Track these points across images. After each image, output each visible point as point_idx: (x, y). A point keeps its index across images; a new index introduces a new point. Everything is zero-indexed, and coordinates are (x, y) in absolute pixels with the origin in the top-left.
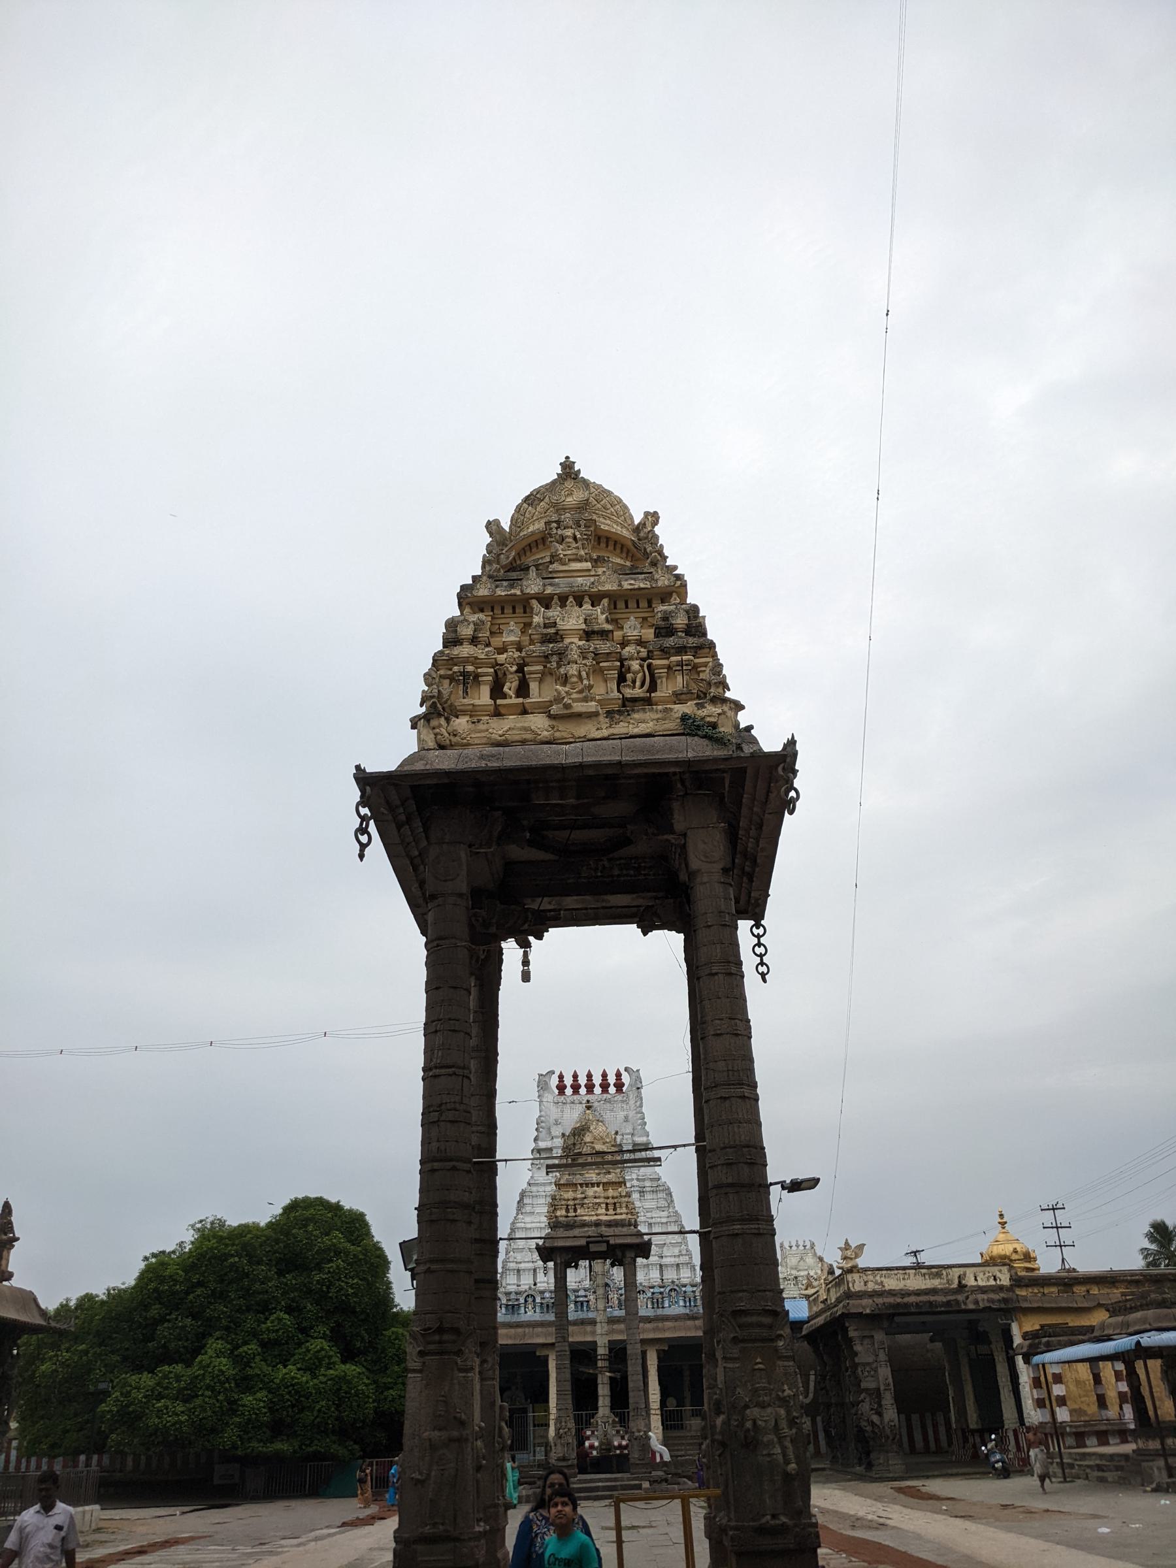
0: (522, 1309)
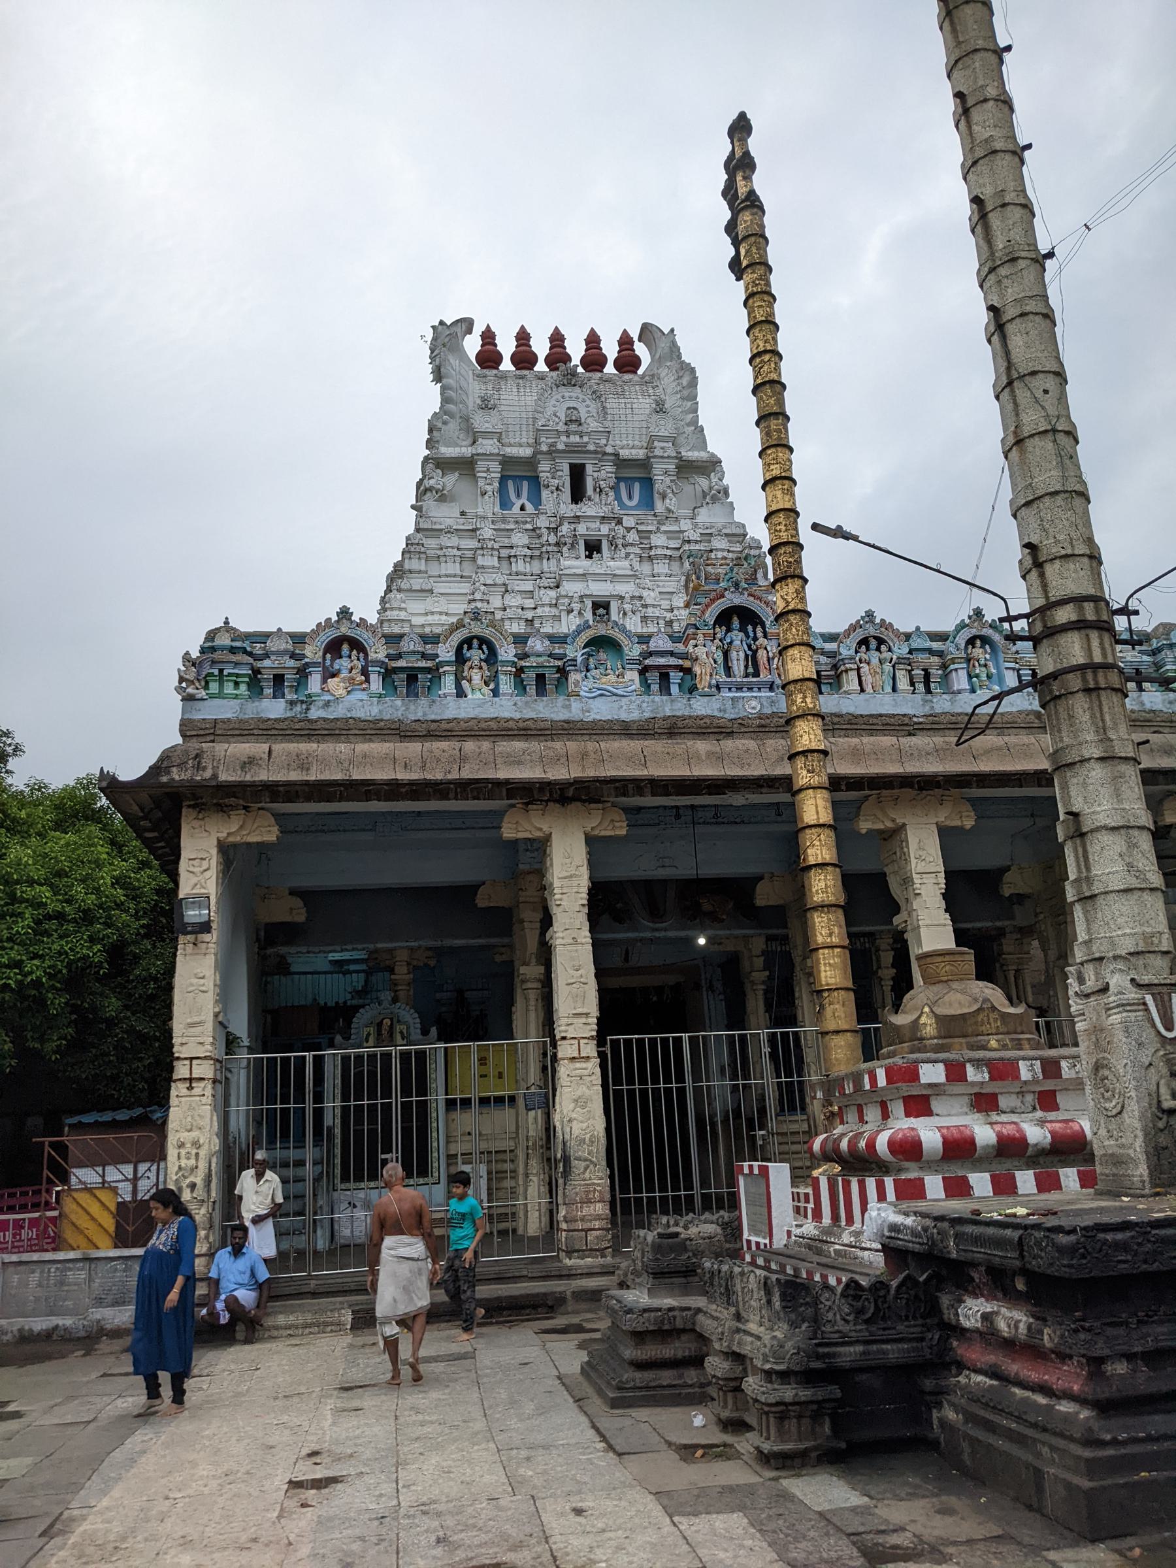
0: (448, 684)
